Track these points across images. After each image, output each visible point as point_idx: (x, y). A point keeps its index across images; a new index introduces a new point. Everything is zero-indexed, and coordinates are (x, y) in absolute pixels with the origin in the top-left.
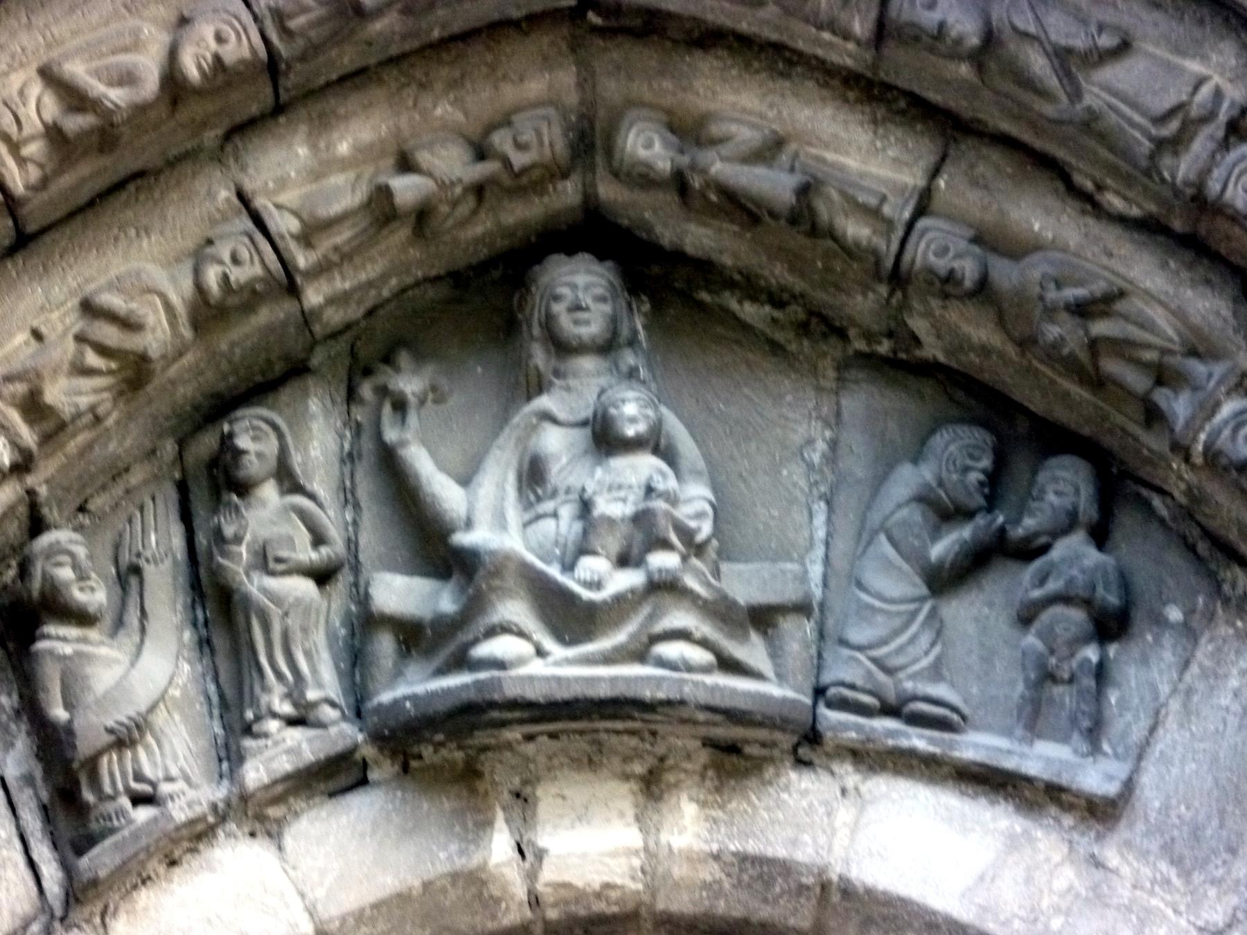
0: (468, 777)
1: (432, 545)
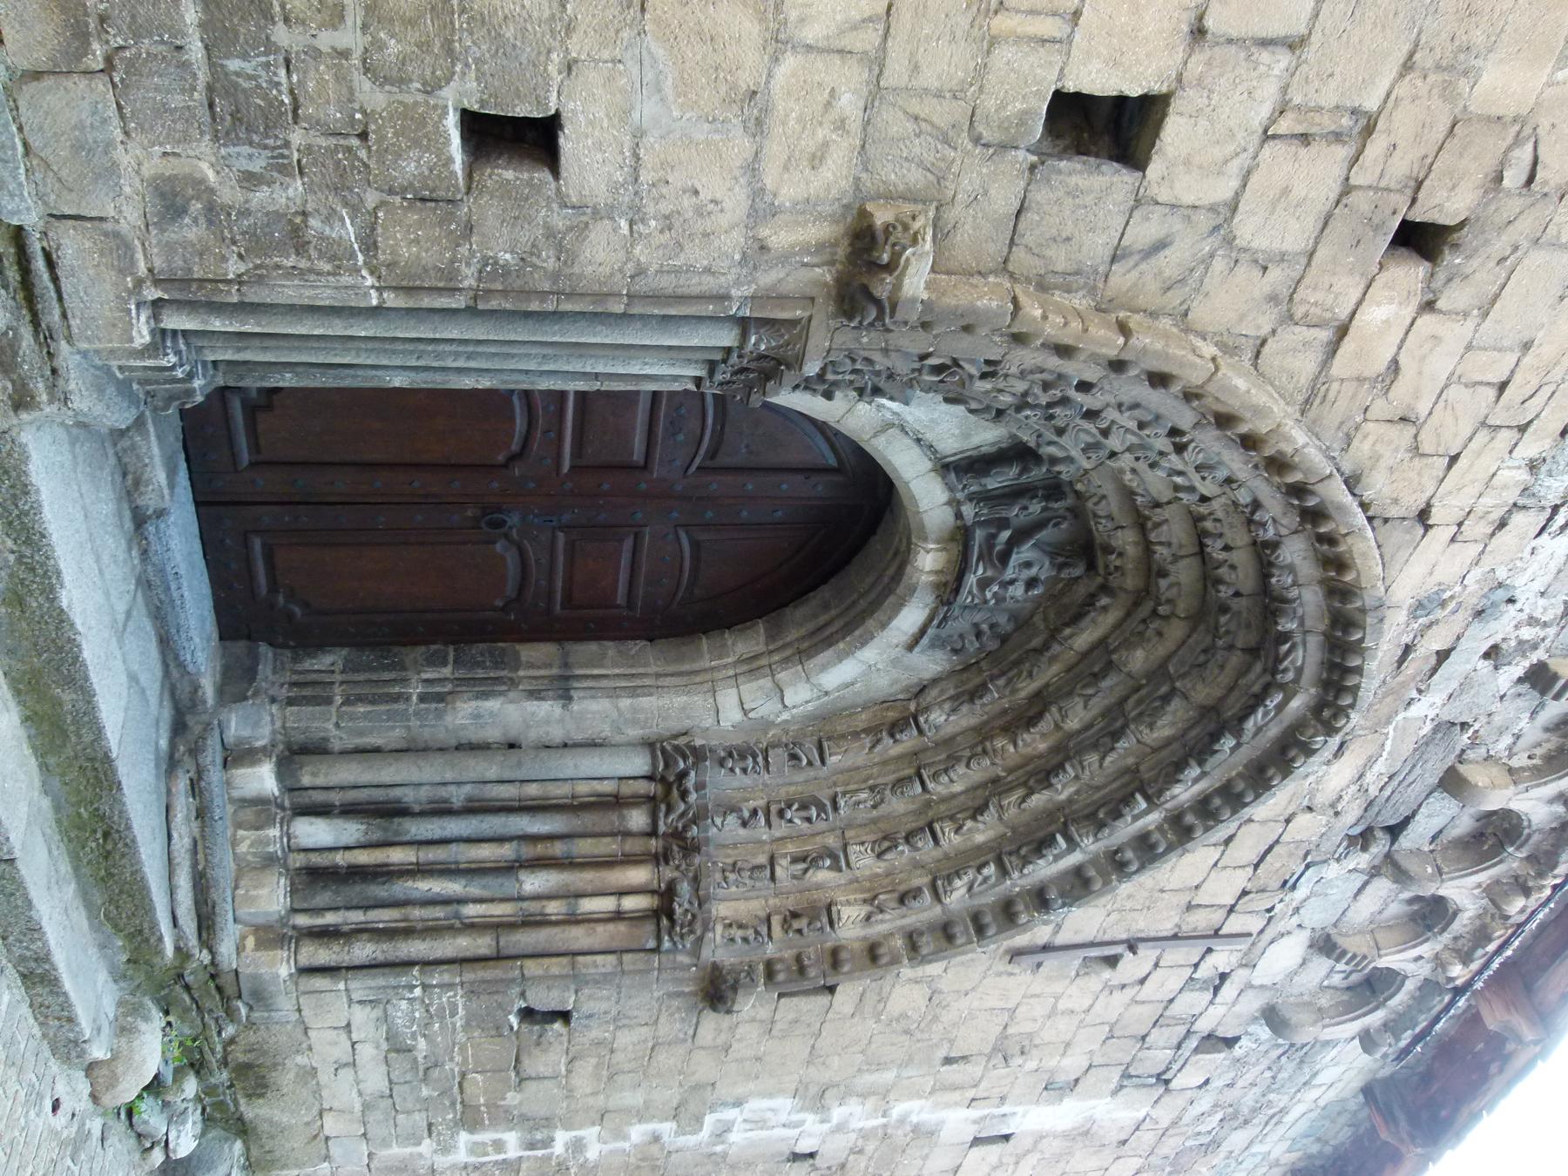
0: (952, 539)
1: (1013, 543)
